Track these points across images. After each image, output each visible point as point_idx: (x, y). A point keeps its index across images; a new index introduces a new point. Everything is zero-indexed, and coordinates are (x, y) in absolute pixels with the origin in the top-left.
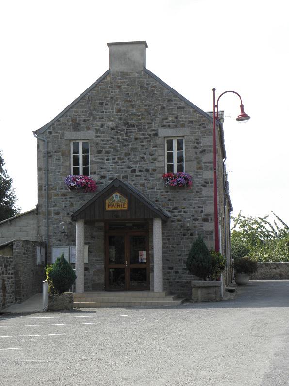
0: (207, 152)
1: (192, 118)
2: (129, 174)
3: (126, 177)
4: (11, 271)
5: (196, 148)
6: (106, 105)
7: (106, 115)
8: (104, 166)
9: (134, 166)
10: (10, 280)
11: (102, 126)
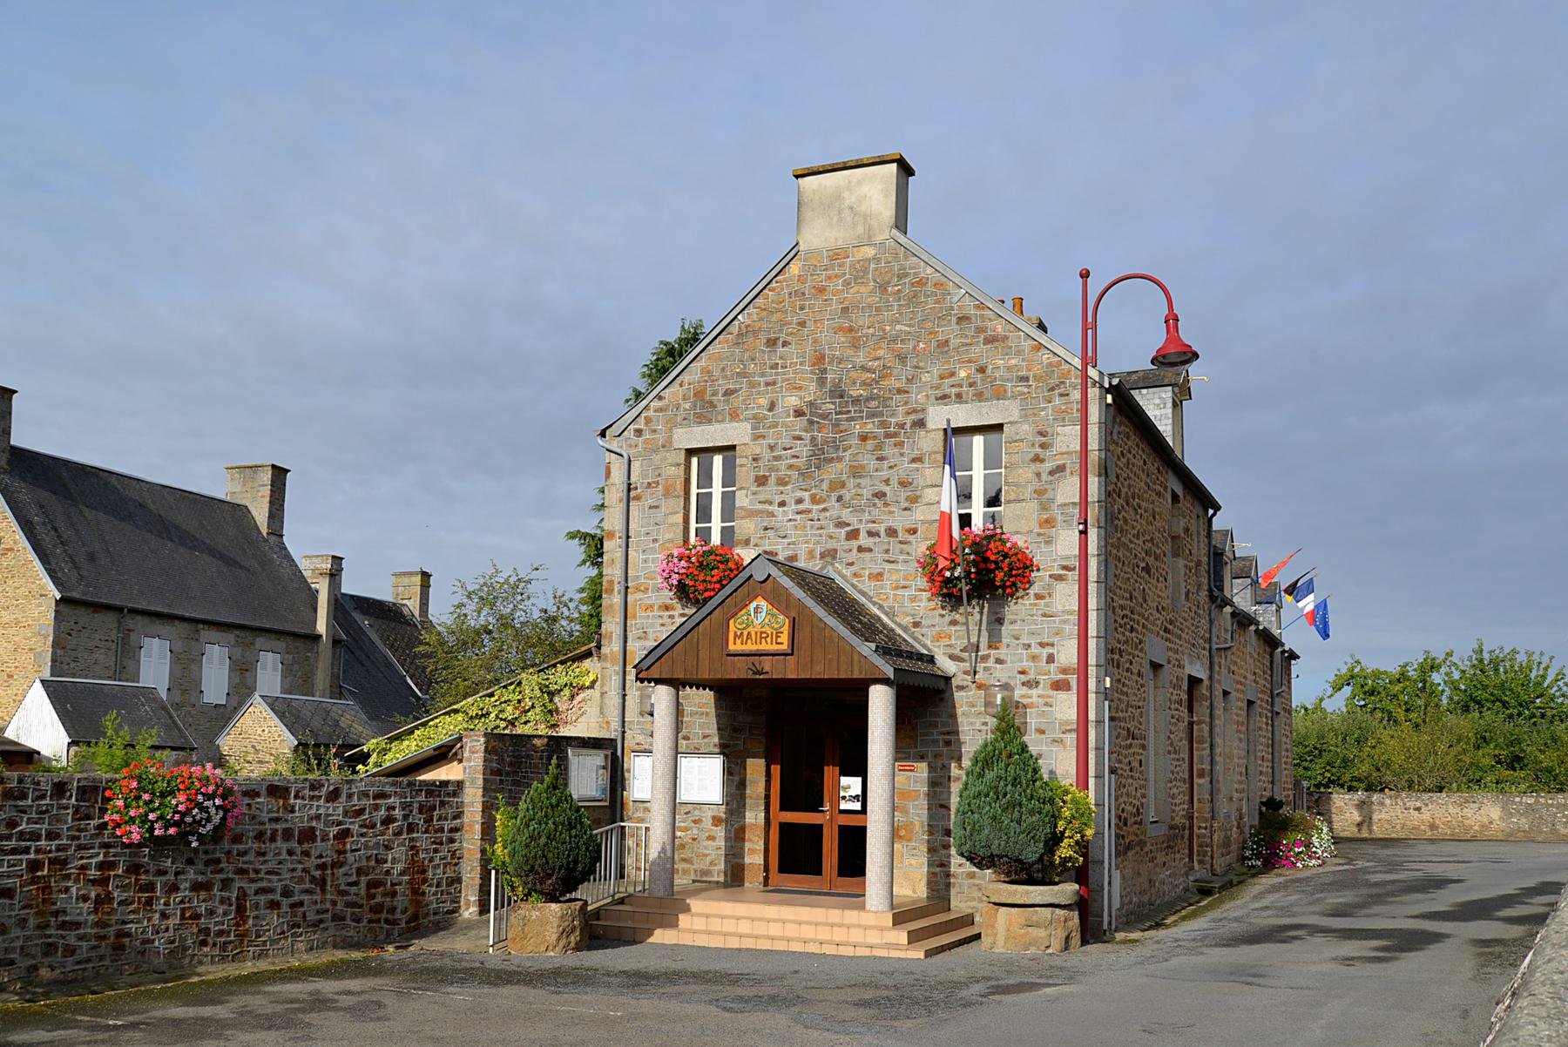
5: (1037, 459)
6: (785, 344)
8: (772, 522)
11: (772, 407)
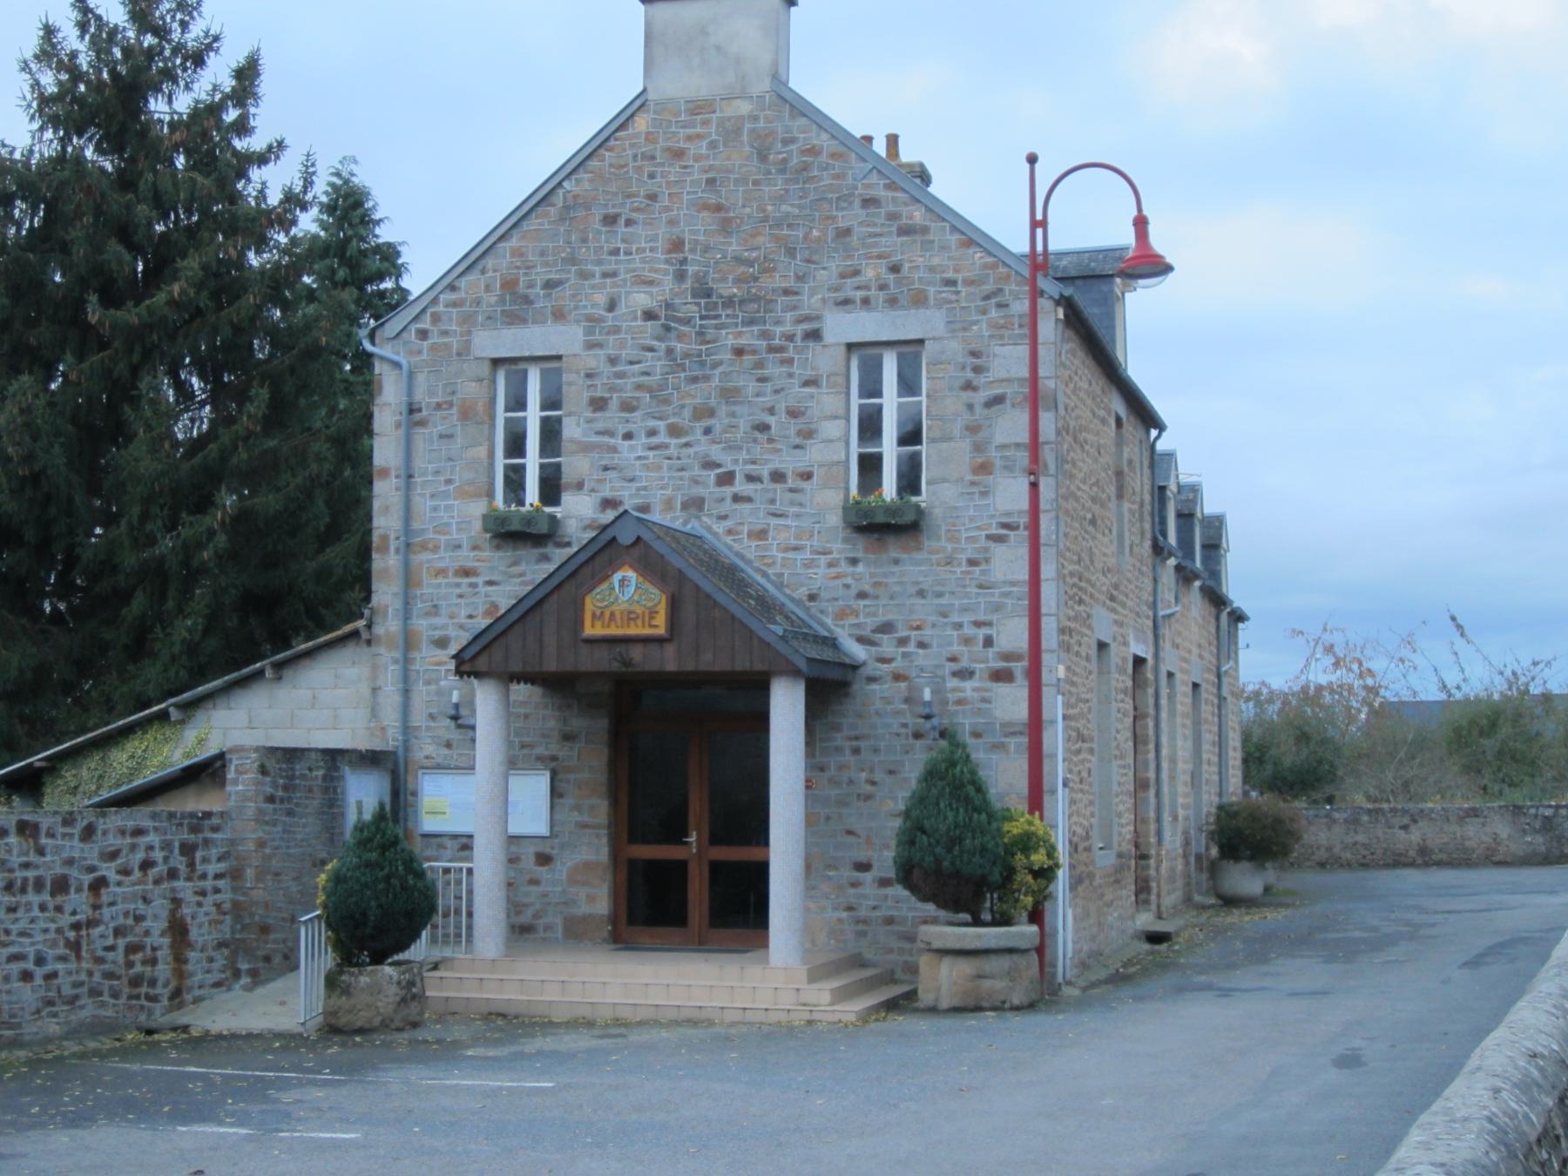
0: (1013, 406)
1: (956, 271)
2: (709, 490)
3: (695, 505)
4: (213, 868)
5: (968, 386)
6: (629, 223)
7: (629, 261)
8: (616, 460)
9: (728, 462)
10: (210, 899)
11: (612, 306)
